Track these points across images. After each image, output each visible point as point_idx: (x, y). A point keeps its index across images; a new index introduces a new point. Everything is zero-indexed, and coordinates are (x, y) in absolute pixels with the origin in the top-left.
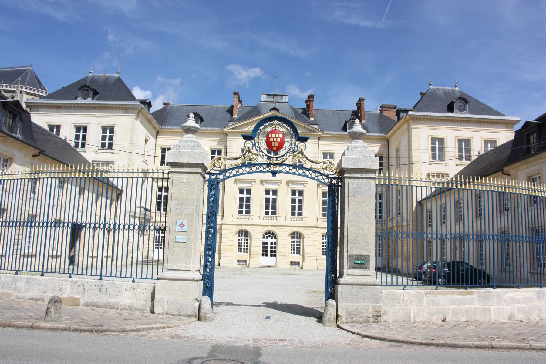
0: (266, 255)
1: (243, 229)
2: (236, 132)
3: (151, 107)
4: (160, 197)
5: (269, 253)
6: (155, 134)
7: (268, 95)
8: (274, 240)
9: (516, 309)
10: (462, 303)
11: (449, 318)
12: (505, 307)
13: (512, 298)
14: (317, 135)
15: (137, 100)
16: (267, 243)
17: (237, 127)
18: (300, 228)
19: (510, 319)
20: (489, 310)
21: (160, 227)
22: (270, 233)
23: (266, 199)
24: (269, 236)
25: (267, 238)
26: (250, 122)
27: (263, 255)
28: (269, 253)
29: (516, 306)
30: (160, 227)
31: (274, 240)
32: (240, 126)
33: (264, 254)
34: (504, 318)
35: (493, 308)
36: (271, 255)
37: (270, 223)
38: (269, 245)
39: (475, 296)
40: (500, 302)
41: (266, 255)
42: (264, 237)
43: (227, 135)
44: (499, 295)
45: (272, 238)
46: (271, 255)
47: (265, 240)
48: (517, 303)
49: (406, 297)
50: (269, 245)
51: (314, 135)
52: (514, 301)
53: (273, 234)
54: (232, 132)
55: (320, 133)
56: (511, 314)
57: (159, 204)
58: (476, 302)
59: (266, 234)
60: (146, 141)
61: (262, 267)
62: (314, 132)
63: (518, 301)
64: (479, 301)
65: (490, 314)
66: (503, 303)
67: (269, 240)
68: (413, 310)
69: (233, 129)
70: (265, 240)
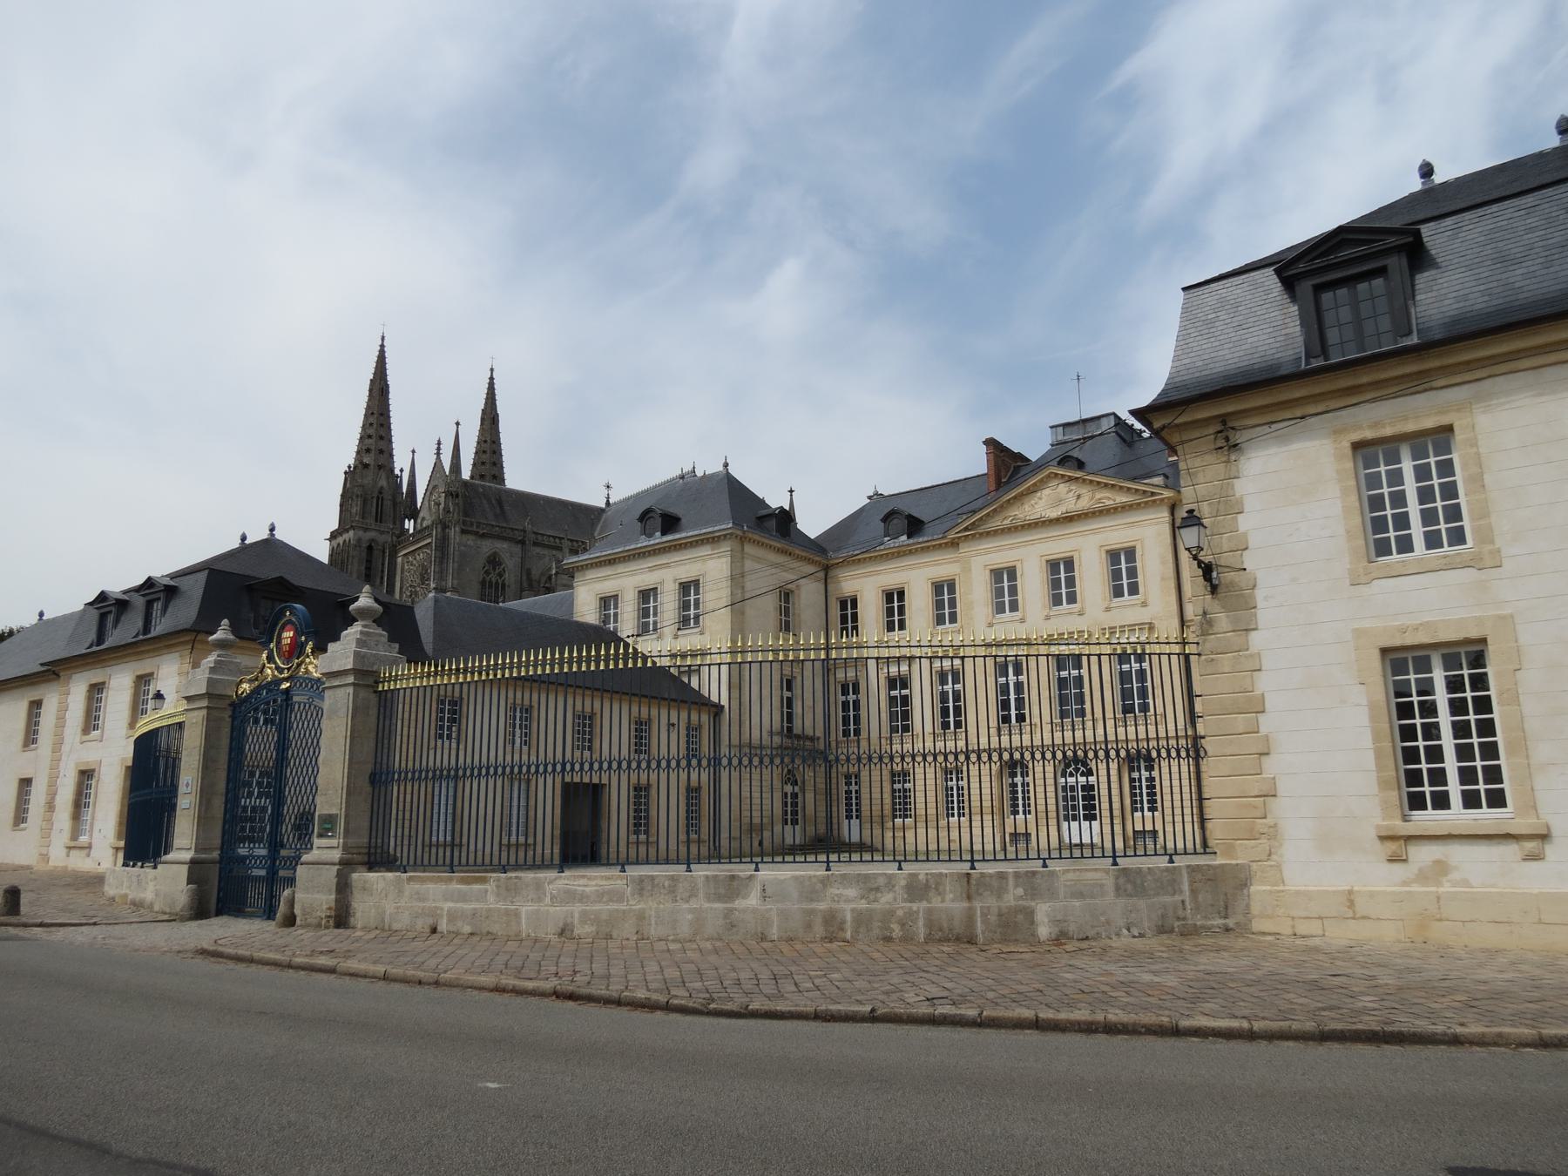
4: (845, 705)
7: (1065, 425)
9: (576, 915)
10: (463, 898)
11: (443, 926)
12: (552, 909)
13: (567, 892)
15: (1042, 464)
19: (562, 933)
20: (517, 914)
21: (1138, 751)
26: (1129, 489)
29: (577, 908)
30: (1138, 751)
34: (549, 932)
35: (526, 909)
39: (490, 887)
40: (540, 900)
44: (539, 886)
48: (580, 901)
49: (381, 885)
52: (571, 896)
56: (566, 925)
58: (491, 898)
63: (583, 898)
64: (498, 895)
65: (519, 923)
66: (548, 900)
68: (389, 907)
69: (966, 529)
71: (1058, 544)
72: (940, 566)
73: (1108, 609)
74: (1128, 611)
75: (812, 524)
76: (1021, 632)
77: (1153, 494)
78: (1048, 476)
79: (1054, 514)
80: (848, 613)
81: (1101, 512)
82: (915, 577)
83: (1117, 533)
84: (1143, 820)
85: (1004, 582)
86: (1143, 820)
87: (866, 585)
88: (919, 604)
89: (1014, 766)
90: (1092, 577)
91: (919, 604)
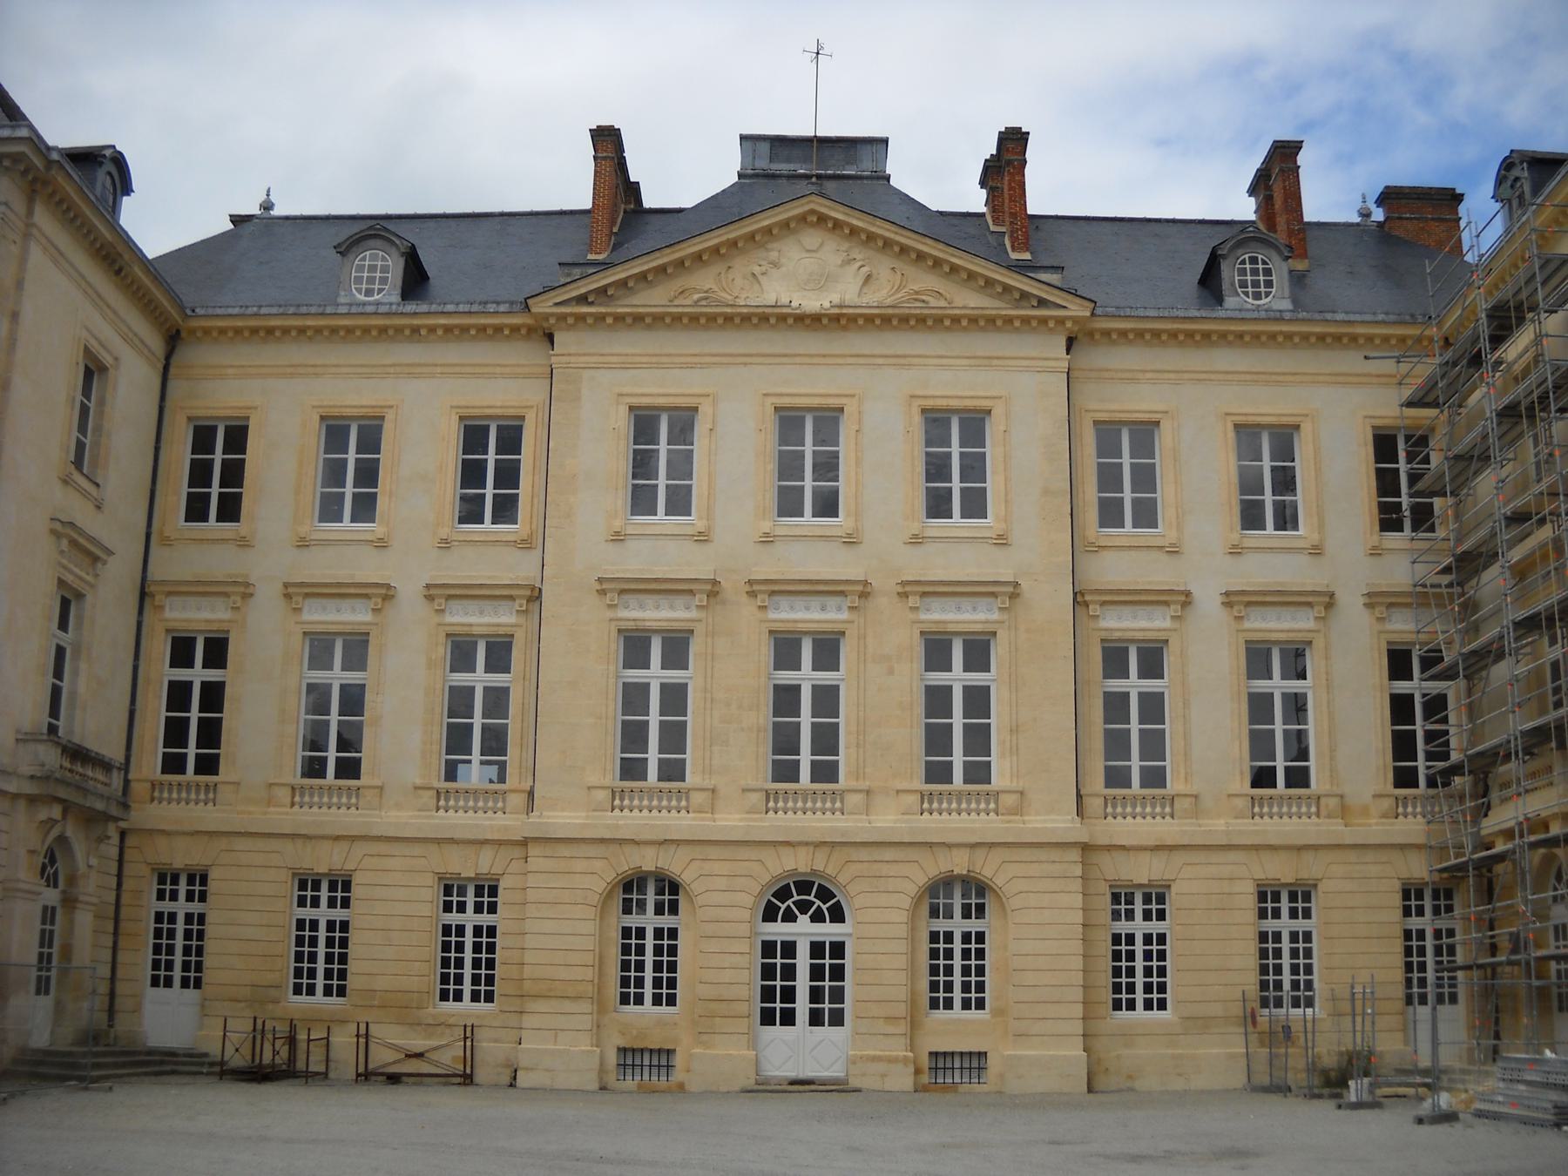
0: (789, 1018)
1: (648, 866)
2: (601, 318)
3: (127, 189)
4: (178, 694)
5: (802, 1005)
6: (157, 344)
8: (828, 931)
14: (1061, 321)
16: (789, 949)
17: (603, 291)
18: (980, 854)
22: (804, 886)
23: (778, 689)
24: (804, 907)
25: (789, 917)
27: (767, 1018)
28: (802, 1005)
31: (828, 931)
32: (623, 283)
33: (775, 1009)
36: (816, 1019)
37: (806, 826)
38: (803, 961)
41: (789, 1018)
42: (770, 914)
43: (550, 338)
45: (818, 918)
46: (816, 1019)
47: (779, 931)
50: (803, 961)
51: (1043, 321)
53: (825, 894)
54: (581, 318)
55: (1078, 309)
57: (175, 732)
59: (783, 893)
60: (93, 372)
61: (763, 1088)
62: (1042, 303)
67: (803, 930)
69: (583, 299)
70: (779, 931)
71: (810, 377)
72: (498, 383)
73: (917, 540)
74: (958, 549)
75: (158, 222)
76: (693, 564)
77: (1042, 303)
78: (802, 219)
79: (813, 303)
80: (217, 473)
81: (921, 320)
82: (424, 406)
83: (952, 373)
84: (954, 1028)
85: (658, 449)
86: (954, 1028)
87: (282, 405)
88: (421, 463)
89: (651, 890)
90: (881, 464)
91: (421, 463)
